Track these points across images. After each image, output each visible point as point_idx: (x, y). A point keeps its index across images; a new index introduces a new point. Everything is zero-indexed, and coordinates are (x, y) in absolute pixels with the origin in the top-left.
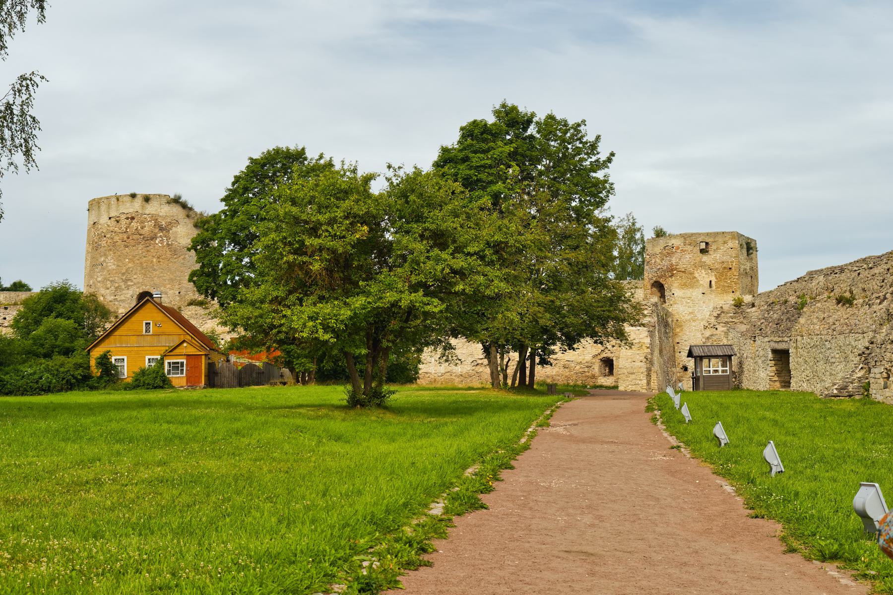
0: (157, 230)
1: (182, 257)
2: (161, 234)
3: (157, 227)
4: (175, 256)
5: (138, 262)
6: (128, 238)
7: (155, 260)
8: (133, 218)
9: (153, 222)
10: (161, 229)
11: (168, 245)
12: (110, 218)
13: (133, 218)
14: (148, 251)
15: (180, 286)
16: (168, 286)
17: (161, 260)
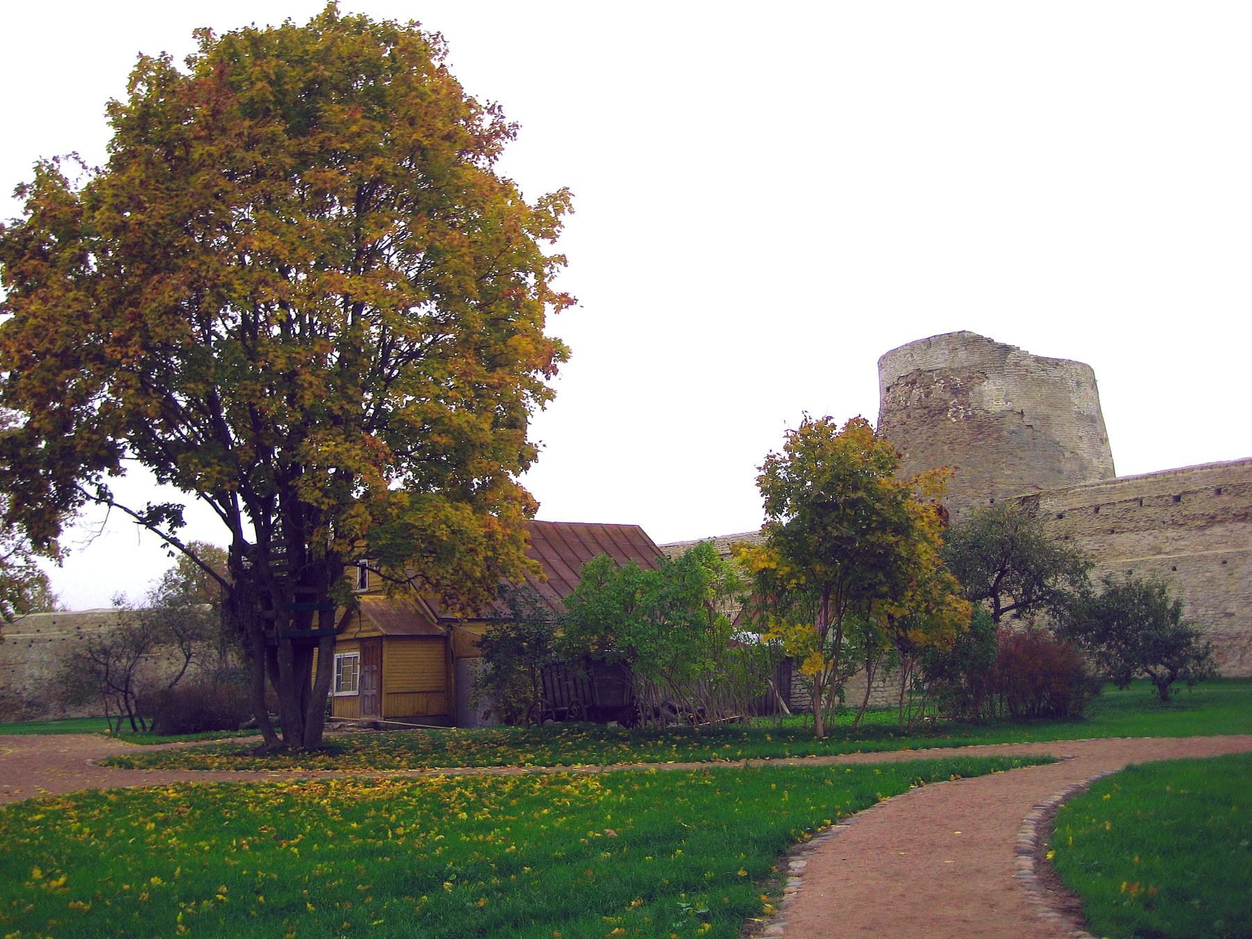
0: (948, 395)
1: (995, 436)
2: (955, 400)
3: (948, 389)
4: (980, 436)
5: (922, 455)
6: (909, 416)
7: (946, 448)
8: (914, 383)
9: (942, 381)
10: (955, 391)
11: (967, 418)
12: (888, 389)
13: (914, 383)
14: (935, 434)
15: (993, 488)
16: (970, 491)
17: (956, 447)
